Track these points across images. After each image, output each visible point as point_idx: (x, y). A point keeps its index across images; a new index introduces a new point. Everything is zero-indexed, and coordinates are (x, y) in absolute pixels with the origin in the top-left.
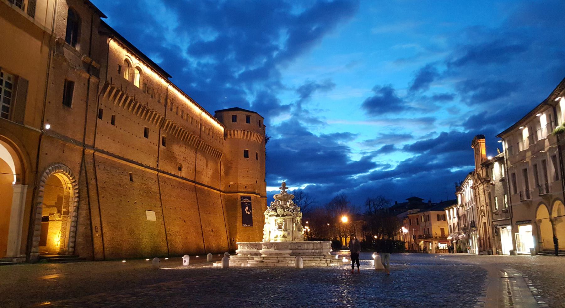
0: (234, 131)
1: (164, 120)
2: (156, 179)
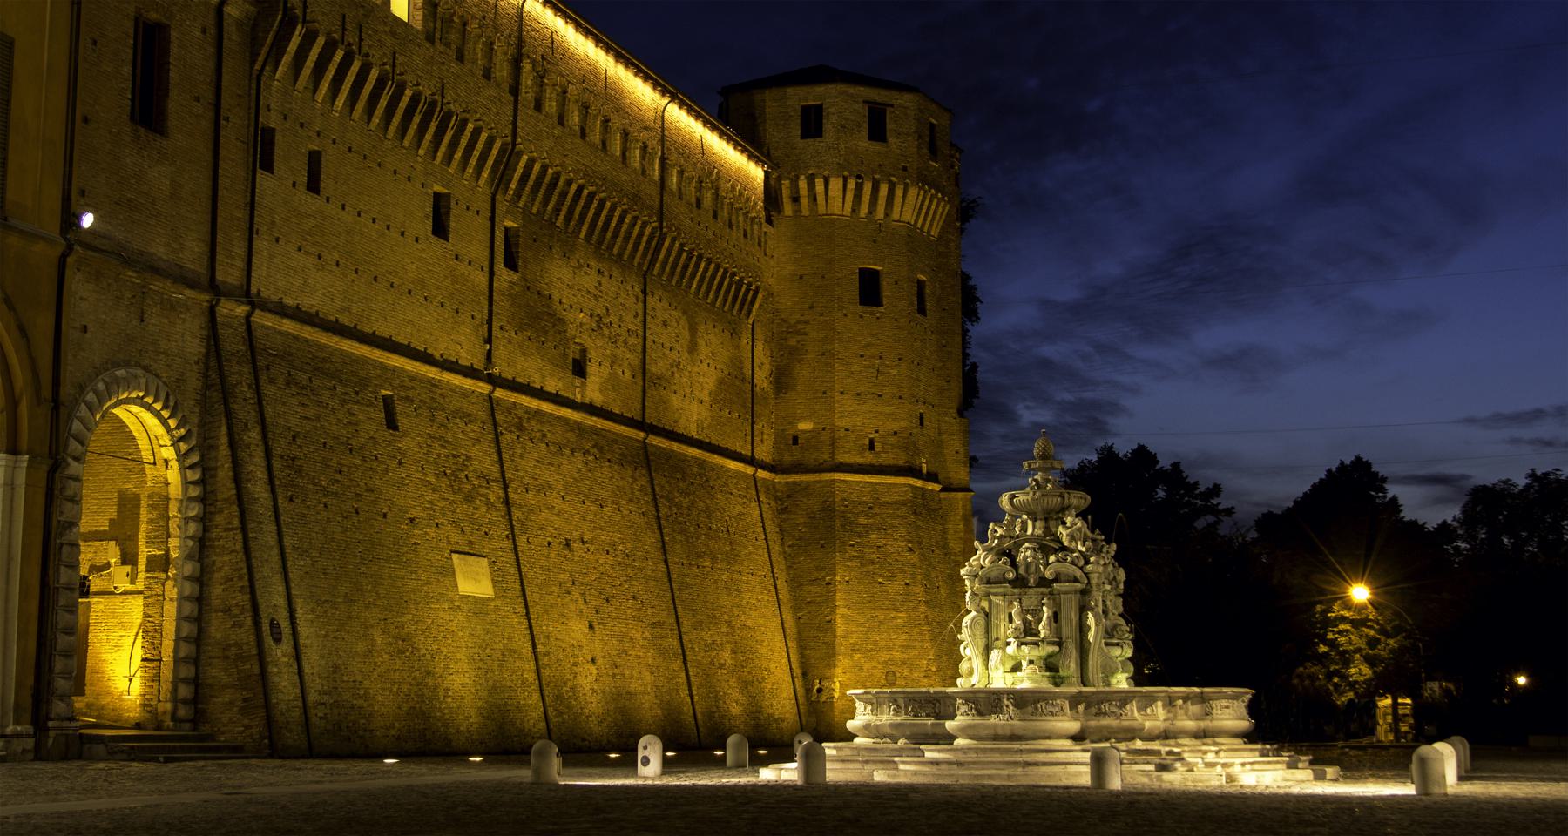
0: (811, 181)
1: (509, 154)
2: (483, 415)
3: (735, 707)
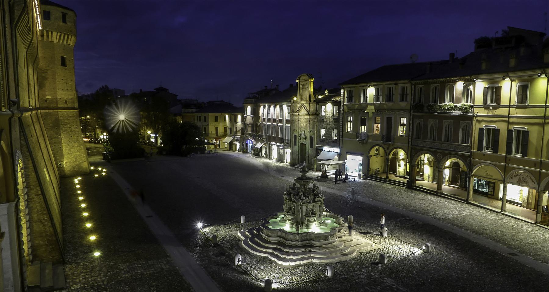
0: (47, 32)
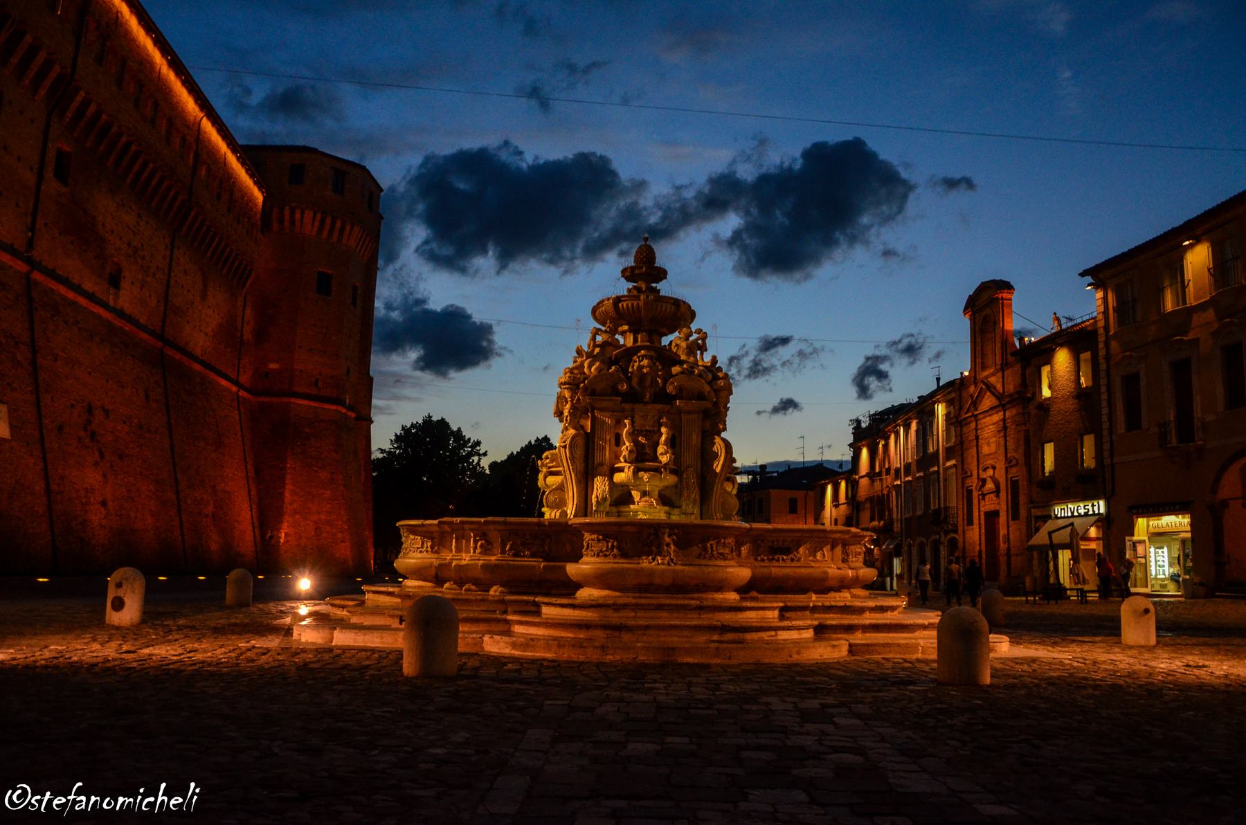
3: (214, 544)
